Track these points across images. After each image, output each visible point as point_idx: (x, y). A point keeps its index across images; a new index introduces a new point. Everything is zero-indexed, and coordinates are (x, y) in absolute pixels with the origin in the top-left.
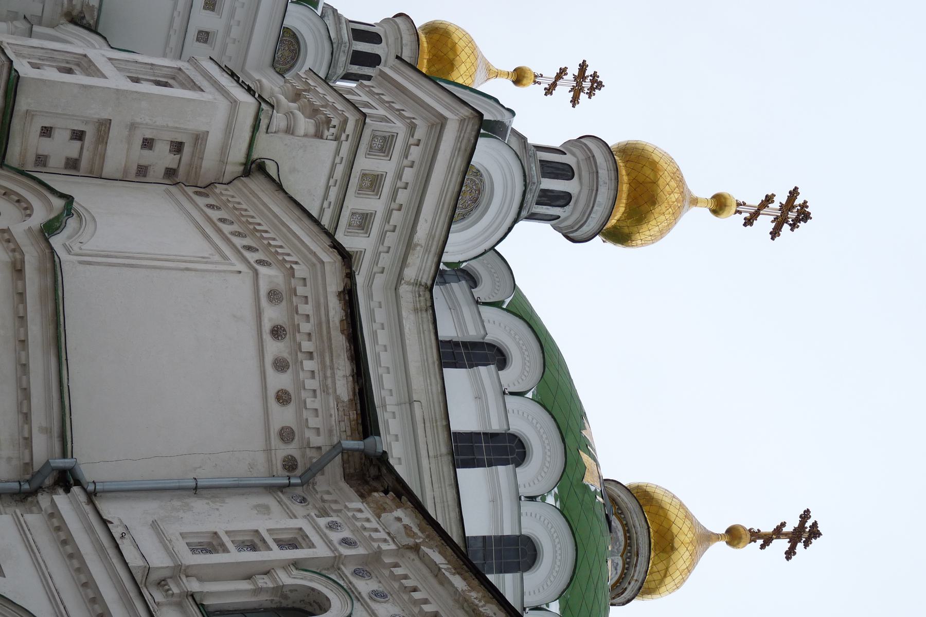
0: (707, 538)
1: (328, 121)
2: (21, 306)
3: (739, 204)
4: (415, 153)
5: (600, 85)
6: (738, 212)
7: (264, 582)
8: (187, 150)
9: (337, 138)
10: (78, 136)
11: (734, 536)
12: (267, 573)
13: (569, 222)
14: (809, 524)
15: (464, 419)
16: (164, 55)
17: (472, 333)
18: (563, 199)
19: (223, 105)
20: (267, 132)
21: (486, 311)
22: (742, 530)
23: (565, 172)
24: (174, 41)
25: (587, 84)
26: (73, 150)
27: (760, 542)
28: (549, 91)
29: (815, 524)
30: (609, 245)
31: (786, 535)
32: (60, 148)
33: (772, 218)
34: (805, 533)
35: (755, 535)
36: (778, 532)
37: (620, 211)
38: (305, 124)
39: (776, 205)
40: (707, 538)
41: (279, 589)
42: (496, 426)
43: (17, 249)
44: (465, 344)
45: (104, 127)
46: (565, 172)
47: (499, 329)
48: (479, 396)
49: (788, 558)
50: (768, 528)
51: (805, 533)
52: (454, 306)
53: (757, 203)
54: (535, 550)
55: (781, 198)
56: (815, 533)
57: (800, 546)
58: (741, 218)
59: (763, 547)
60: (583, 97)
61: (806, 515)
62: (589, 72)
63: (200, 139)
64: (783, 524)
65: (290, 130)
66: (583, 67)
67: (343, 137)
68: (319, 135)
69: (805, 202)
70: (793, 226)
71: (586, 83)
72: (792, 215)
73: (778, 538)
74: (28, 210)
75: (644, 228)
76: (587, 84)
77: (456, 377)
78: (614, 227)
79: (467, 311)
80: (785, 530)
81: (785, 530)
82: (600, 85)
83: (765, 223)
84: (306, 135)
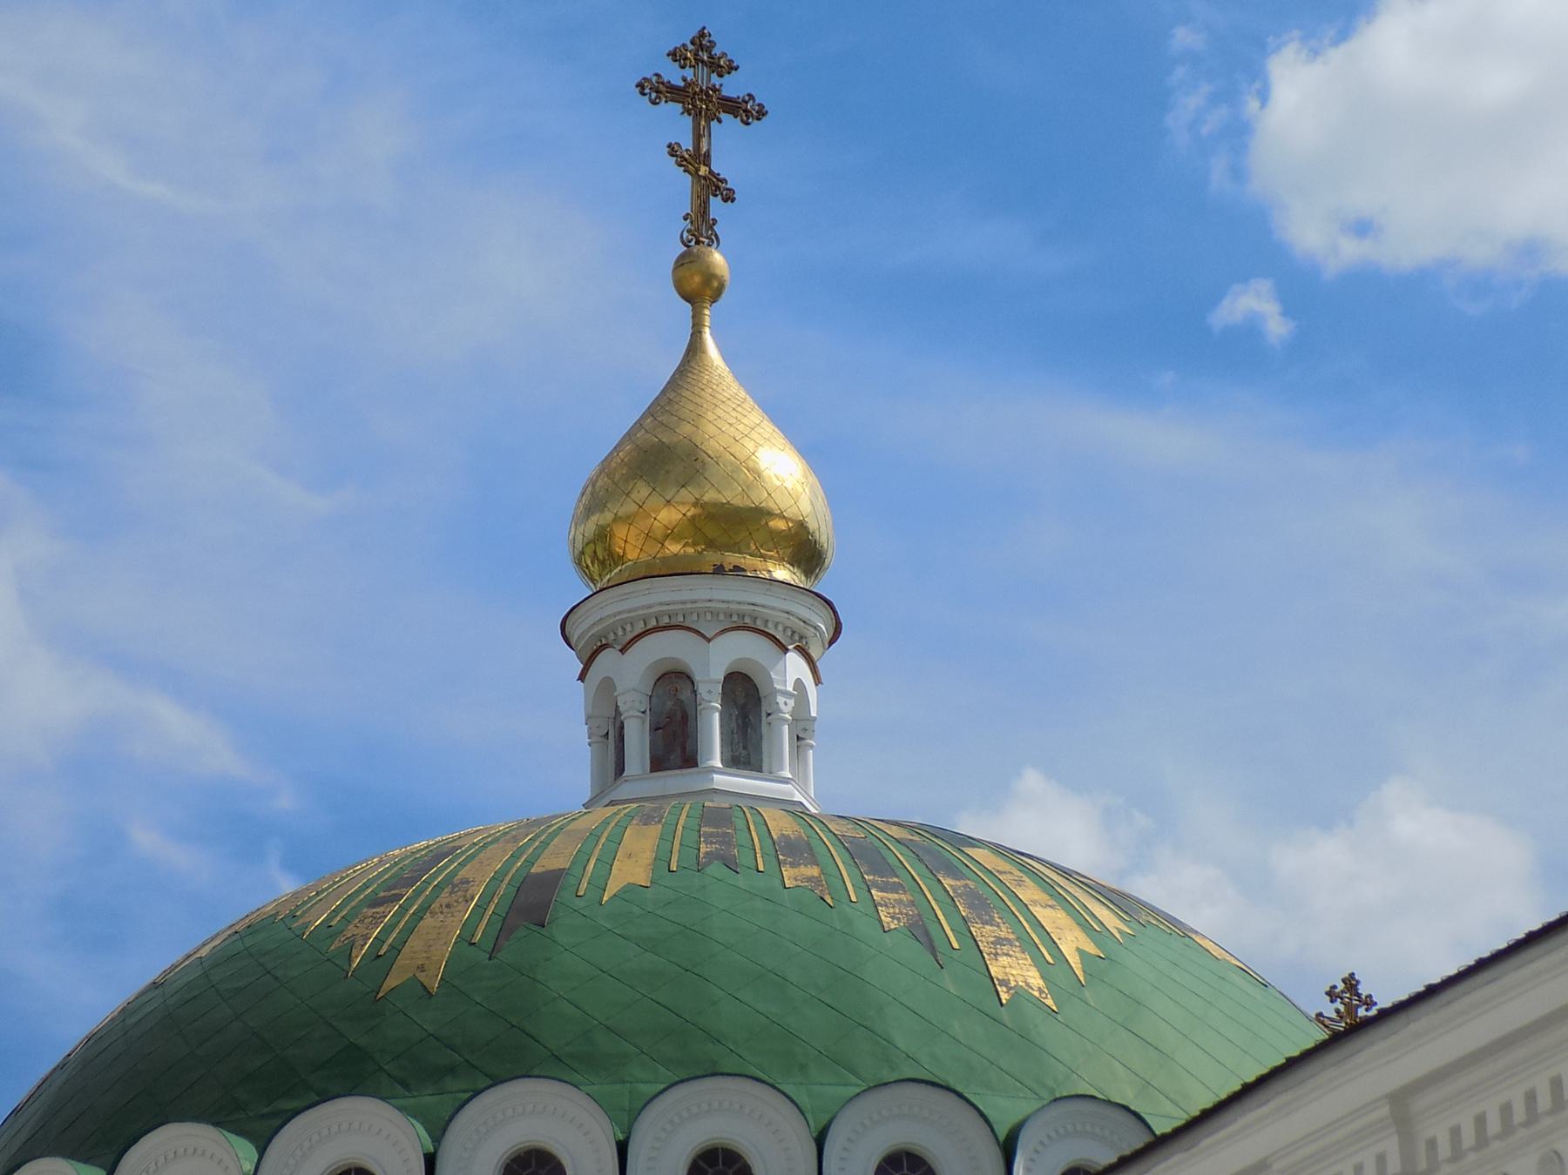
27: (715, 203)
29: (673, 55)
31: (698, 137)
35: (701, 229)
36: (693, 160)
49: (761, 113)
50: (683, 182)
51: (699, 88)
56: (700, 51)
57: (732, 86)
59: (729, 197)
61: (656, 90)
73: (706, 159)
80: (687, 144)
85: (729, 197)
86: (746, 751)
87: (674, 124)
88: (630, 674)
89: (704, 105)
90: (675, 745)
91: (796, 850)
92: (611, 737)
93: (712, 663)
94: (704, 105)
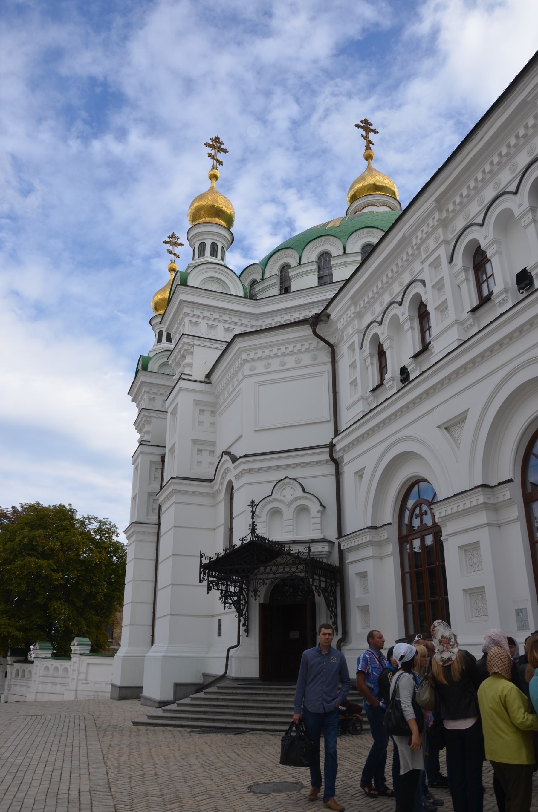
1: (186, 350)
2: (263, 469)
3: (213, 168)
4: (197, 312)
5: (173, 234)
6: (216, 169)
7: (369, 361)
8: (202, 408)
9: (193, 345)
10: (200, 451)
12: (365, 361)
13: (224, 243)
14: (361, 124)
15: (312, 280)
16: (167, 419)
17: (276, 280)
18: (214, 246)
19: (181, 393)
20: (191, 375)
21: (267, 275)
22: (366, 154)
23: (202, 246)
24: (161, 415)
25: (173, 240)
26: (205, 454)
27: (371, 145)
28: (177, 256)
29: (361, 122)
30: (235, 223)
31: (367, 134)
32: (205, 457)
33: (218, 153)
35: (368, 148)
36: (366, 138)
37: (217, 220)
38: (188, 360)
39: (213, 152)
40: (369, 169)
41: (371, 355)
42: (315, 267)
43: (241, 472)
44: (281, 283)
46: (202, 246)
47: (273, 269)
49: (378, 132)
50: (364, 142)
51: (366, 126)
52: (265, 289)
53: (212, 160)
54: (367, 245)
55: (209, 150)
56: (365, 121)
57: (371, 127)
58: (219, 167)
59: (373, 144)
60: (179, 241)
61: (358, 126)
62: (168, 240)
64: (362, 136)
65: (191, 365)
66: (166, 243)
67: (192, 343)
68: (192, 353)
69: (210, 139)
70: (222, 143)
71: (173, 240)
72: (217, 144)
73: (368, 137)
74: (228, 469)
75: (225, 209)
76: (173, 240)
77: (295, 286)
78: (225, 222)
79: (267, 284)
80: (365, 135)
81: (365, 135)
82: (173, 234)
83: (221, 156)
84: (192, 359)
85: (373, 144)
87: (362, 132)
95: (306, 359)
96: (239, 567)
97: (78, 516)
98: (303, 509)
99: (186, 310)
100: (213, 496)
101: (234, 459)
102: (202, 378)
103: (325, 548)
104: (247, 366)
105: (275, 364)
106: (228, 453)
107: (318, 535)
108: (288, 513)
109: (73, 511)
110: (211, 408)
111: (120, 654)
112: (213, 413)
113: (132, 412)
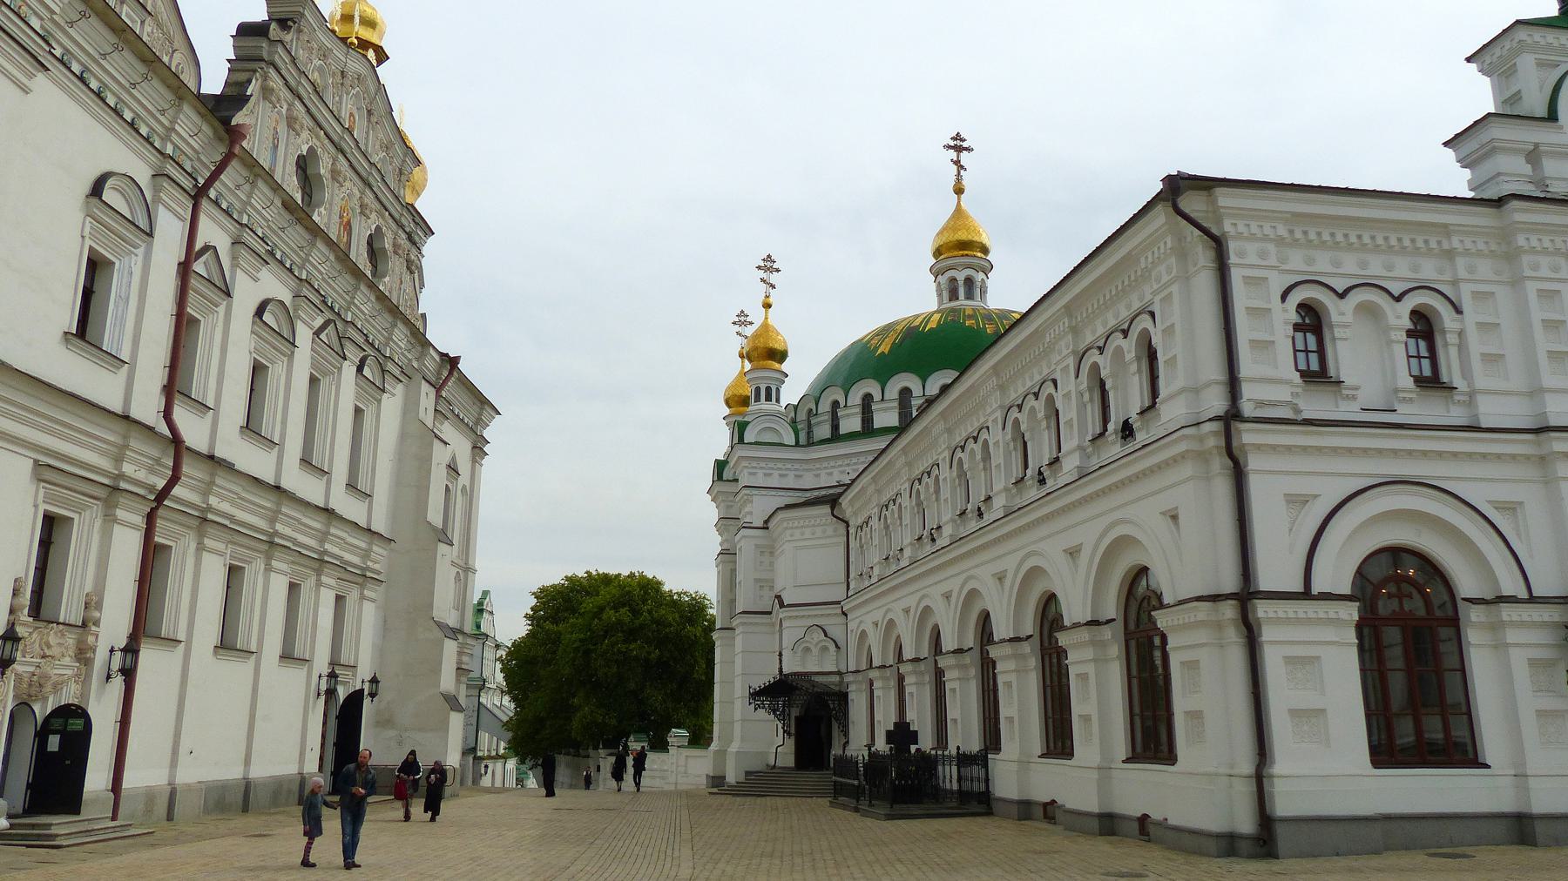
0: (959, 212)
11: (959, 191)
17: (827, 417)
18: (768, 390)
34: (958, 146)
36: (957, 163)
40: (959, 212)
42: (858, 410)
45: (757, 581)
47: (825, 406)
48: (848, 416)
55: (761, 274)
56: (958, 137)
57: (965, 145)
61: (949, 147)
63: (757, 546)
83: (774, 278)
86: (970, 296)
87: (953, 154)
88: (943, 279)
89: (959, 149)
90: (954, 295)
91: (970, 317)
92: (940, 295)
93: (961, 276)
94: (959, 149)
95: (830, 531)
96: (779, 692)
97: (666, 588)
98: (825, 649)
99: (745, 463)
100: (773, 625)
101: (782, 605)
102: (761, 524)
103: (836, 679)
104: (788, 532)
105: (808, 532)
106: (778, 597)
107: (834, 669)
108: (815, 651)
109: (659, 583)
110: (769, 551)
111: (714, 746)
112: (772, 553)
113: (711, 513)
